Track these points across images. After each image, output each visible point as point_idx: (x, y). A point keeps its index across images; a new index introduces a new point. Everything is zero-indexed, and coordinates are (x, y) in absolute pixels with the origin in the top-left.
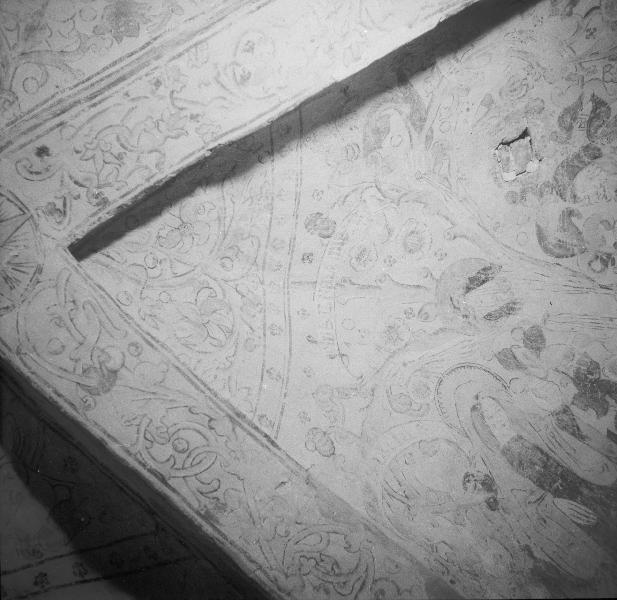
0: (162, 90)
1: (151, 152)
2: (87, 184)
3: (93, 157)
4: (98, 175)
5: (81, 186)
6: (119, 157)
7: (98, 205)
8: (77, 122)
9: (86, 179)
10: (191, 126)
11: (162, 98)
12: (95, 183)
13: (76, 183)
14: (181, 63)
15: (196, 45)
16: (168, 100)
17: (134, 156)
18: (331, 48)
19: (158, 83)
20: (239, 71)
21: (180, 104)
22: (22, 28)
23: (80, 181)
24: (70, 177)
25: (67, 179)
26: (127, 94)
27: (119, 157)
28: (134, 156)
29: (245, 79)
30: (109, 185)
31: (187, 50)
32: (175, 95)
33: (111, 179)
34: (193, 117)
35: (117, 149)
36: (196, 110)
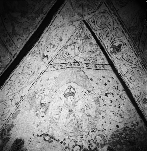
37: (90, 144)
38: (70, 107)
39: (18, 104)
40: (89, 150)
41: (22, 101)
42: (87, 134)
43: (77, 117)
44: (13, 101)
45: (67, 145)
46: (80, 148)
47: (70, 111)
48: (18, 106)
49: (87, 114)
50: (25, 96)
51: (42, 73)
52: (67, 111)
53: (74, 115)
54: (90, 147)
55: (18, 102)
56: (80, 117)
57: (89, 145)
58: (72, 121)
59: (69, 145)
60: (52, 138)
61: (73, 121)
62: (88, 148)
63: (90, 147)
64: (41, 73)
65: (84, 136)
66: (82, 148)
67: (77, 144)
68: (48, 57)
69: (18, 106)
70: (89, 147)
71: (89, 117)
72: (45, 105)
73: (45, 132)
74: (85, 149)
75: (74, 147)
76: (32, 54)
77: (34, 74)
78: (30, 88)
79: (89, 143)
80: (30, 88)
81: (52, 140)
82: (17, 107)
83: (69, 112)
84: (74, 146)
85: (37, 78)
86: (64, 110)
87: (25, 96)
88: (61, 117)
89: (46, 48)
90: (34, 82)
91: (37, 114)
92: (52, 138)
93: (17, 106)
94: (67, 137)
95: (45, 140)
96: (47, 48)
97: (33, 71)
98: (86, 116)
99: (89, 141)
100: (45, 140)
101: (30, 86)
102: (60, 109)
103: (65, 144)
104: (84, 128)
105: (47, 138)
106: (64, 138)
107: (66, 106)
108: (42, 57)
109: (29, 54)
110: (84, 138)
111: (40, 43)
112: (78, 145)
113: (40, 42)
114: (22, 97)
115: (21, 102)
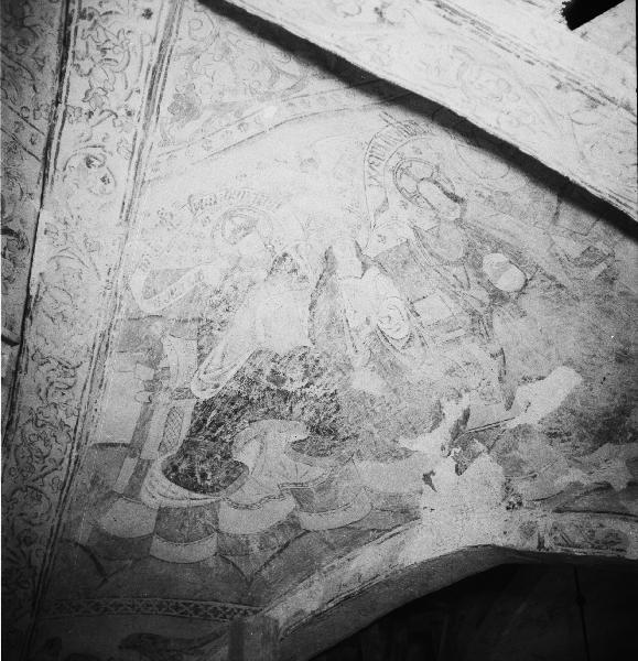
0: (122, 112)
1: (90, 71)
2: (104, 17)
3: (118, 37)
4: (104, 29)
5: (106, 13)
6: (104, 51)
7: (85, 10)
8: (147, 50)
9: (107, 19)
10: (86, 107)
11: (118, 108)
12: (100, 23)
13: (111, 12)
14: (130, 138)
15: (133, 153)
16: (115, 111)
17: (97, 60)
18: (66, 223)
19: (129, 114)
20: (96, 163)
21: (106, 114)
22: (232, 47)
23: (109, 16)
24: (117, 13)
25: (121, 12)
26: (138, 91)
27: (104, 51)
28: (97, 60)
29: (89, 163)
30: (91, 29)
31: (134, 147)
32: (113, 117)
33: (94, 33)
34: (90, 114)
35: (109, 54)
36: (94, 120)
39: (592, 99)
41: (579, 84)
44: (577, 117)
48: (603, 100)
51: (447, 15)
55: (586, 97)
64: (448, 19)
68: (378, 5)
69: (603, 100)
76: (383, 65)
77: (458, 49)
78: (518, 57)
80: (518, 57)
85: (474, 36)
87: (553, 77)
89: (349, 18)
90: (492, 42)
96: (347, 14)
97: (451, 53)
101: (511, 58)
108: (384, 29)
109: (388, 74)
111: (339, 43)
113: (338, 46)
114: (559, 87)
115: (586, 88)
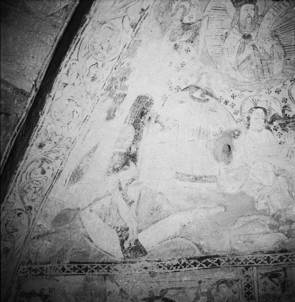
37: (285, 107)
38: (245, 28)
39: (136, 25)
40: (282, 117)
41: (144, 19)
42: (281, 85)
43: (261, 50)
45: (237, 108)
46: (264, 114)
47: (244, 37)
48: (136, 30)
49: (283, 43)
50: (148, 8)
52: (239, 37)
53: (254, 46)
54: (286, 112)
55: (136, 22)
56: (268, 50)
57: (283, 108)
58: (249, 58)
59: (241, 108)
60: (207, 93)
61: (252, 58)
62: (281, 114)
63: (286, 112)
65: (273, 90)
66: (268, 114)
67: (258, 106)
69: (136, 30)
70: (283, 111)
71: (286, 50)
72: (191, 26)
73: (192, 81)
74: (274, 115)
75: (251, 111)
79: (283, 104)
81: (207, 97)
82: (135, 32)
83: (243, 40)
84: (253, 110)
86: (231, 35)
87: (148, 8)
88: (225, 51)
91: (176, 47)
92: (207, 93)
93: (134, 31)
94: (237, 92)
95: (194, 98)
98: (280, 47)
99: (285, 100)
100: (194, 98)
102: (224, 34)
103: (233, 106)
104: (275, 73)
105: (197, 94)
106: (231, 94)
107: (237, 27)
110: (273, 94)
112: (262, 108)
114: (143, 10)
115: (142, 22)
